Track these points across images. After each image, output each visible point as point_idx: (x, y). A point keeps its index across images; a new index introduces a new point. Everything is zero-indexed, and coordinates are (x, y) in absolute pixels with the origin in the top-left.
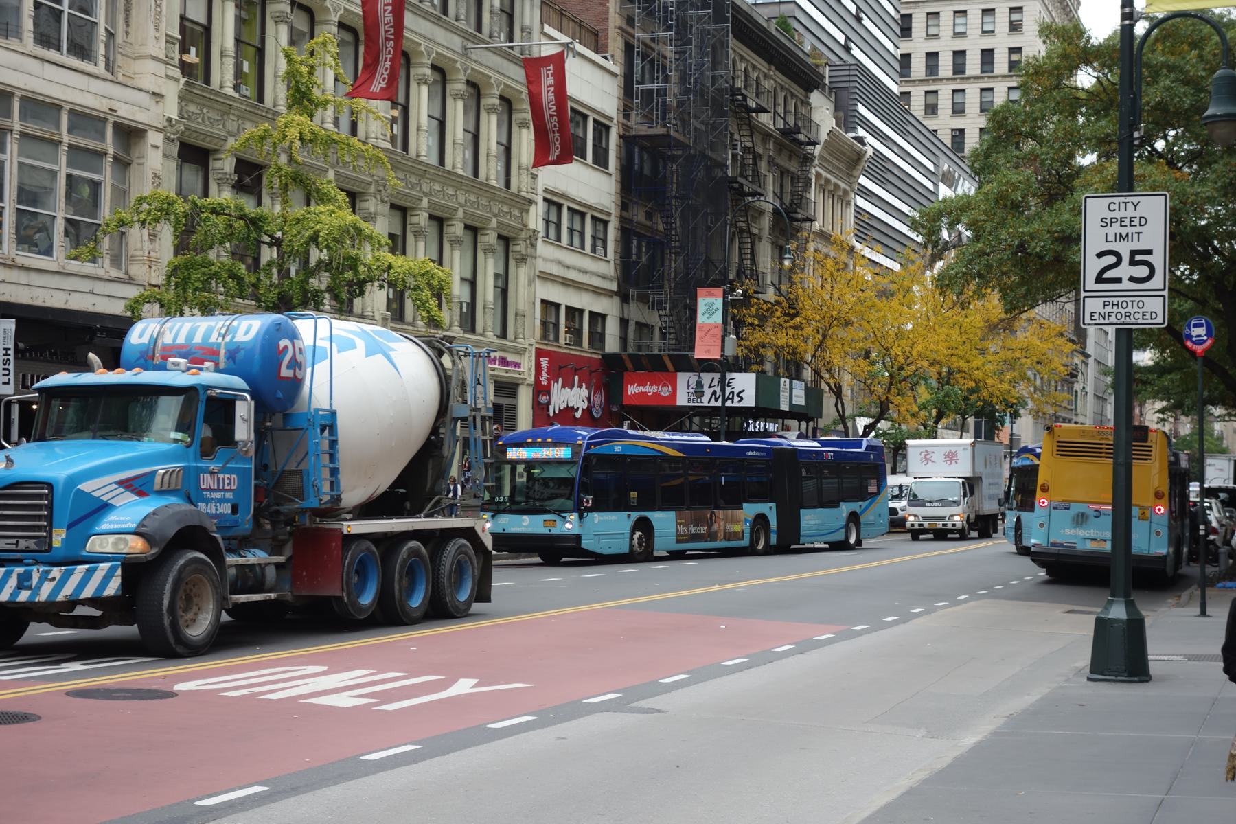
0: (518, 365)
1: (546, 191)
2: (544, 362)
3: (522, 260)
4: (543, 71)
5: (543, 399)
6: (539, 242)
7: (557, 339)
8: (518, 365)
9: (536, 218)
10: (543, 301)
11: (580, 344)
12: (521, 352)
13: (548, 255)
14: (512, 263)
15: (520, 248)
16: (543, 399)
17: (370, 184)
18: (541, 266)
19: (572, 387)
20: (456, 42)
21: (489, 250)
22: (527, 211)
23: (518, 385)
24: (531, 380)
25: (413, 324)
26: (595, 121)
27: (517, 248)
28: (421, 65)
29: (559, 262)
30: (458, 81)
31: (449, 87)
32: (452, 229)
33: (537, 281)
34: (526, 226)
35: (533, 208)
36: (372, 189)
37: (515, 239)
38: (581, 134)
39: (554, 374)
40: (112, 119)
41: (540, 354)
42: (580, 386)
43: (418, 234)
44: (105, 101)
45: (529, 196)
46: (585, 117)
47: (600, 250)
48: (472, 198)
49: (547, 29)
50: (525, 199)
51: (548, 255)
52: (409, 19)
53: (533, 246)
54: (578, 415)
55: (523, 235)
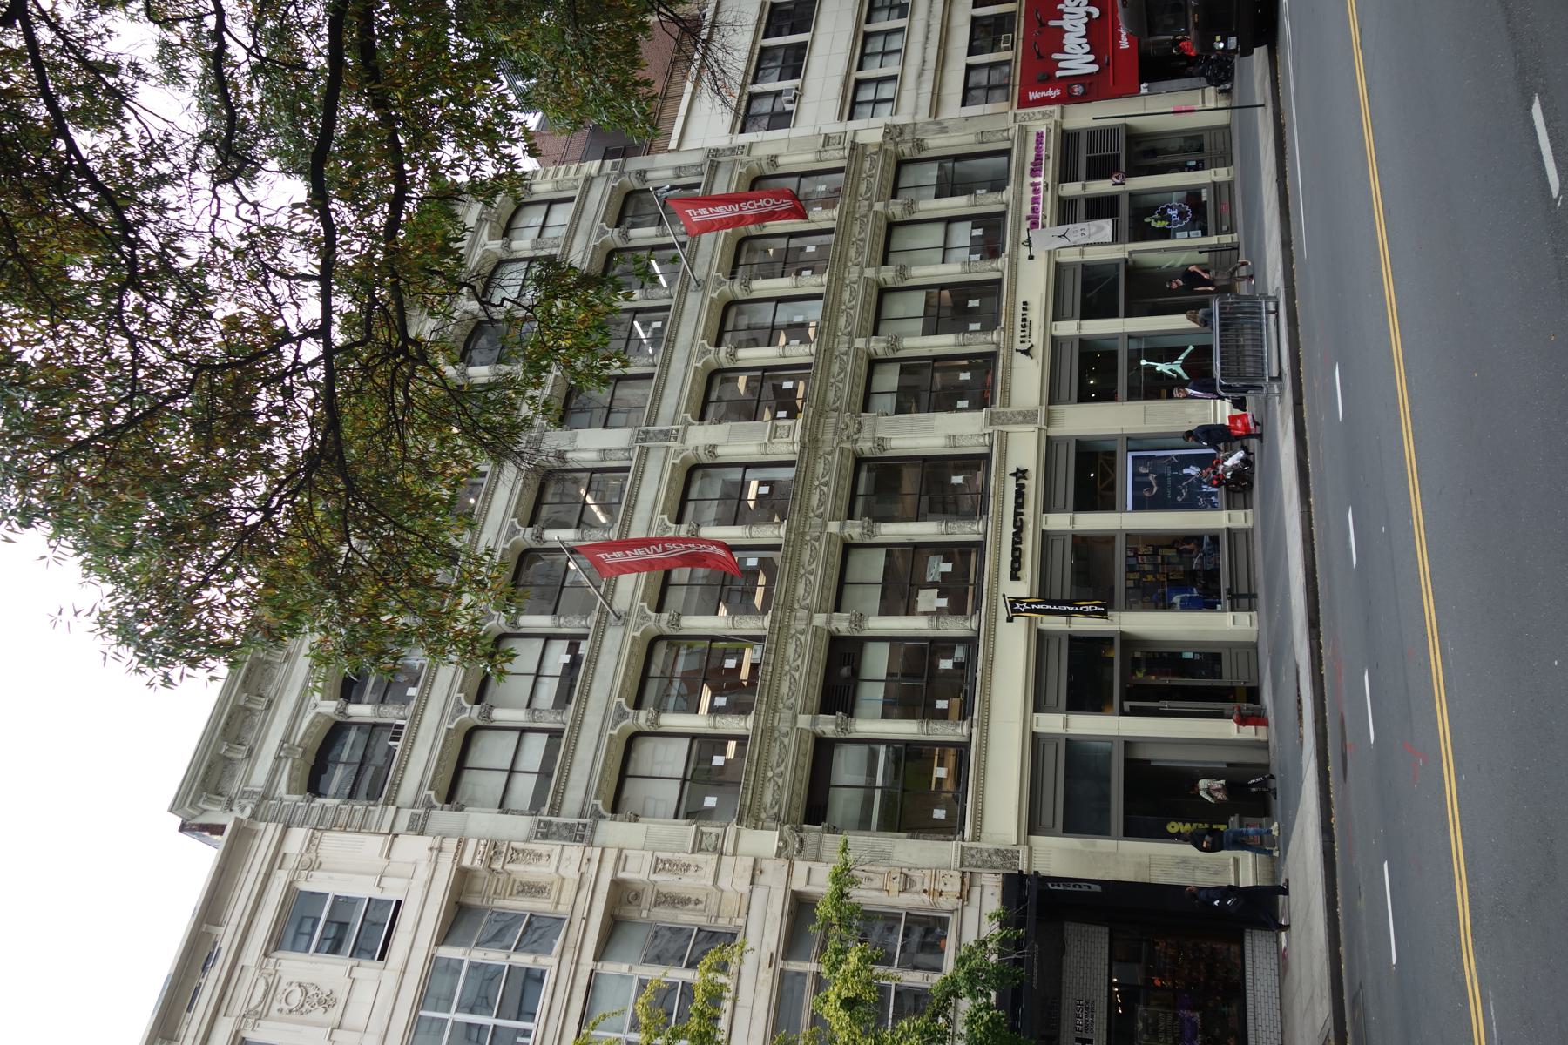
0: (1040, 135)
1: (840, 118)
2: (1033, 96)
3: (919, 145)
4: (696, 219)
5: (1078, 90)
6: (902, 118)
7: (1008, 63)
8: (1040, 135)
9: (870, 130)
10: (963, 105)
11: (1011, 15)
12: (1023, 130)
13: (911, 107)
14: (924, 155)
15: (906, 149)
16: (1078, 90)
17: (842, 449)
18: (923, 116)
19: (1061, 31)
20: (693, 300)
21: (910, 206)
22: (865, 145)
23: (1063, 131)
24: (1056, 108)
25: (998, 345)
26: (765, 37)
27: (907, 151)
28: (717, 359)
29: (920, 75)
30: (732, 290)
31: (741, 297)
32: (889, 280)
33: (940, 118)
34: (881, 146)
35: (860, 139)
36: (847, 445)
37: (897, 155)
38: (781, 53)
39: (1048, 80)
40: (781, 963)
41: (1024, 103)
42: (1060, 15)
43: (894, 345)
44: (762, 976)
45: (848, 146)
46: (763, 49)
47: (896, 42)
48: (852, 253)
49: (673, 145)
50: (852, 149)
51: (911, 107)
52: (637, 532)
53: (901, 129)
54: (1096, 12)
55: (891, 147)
